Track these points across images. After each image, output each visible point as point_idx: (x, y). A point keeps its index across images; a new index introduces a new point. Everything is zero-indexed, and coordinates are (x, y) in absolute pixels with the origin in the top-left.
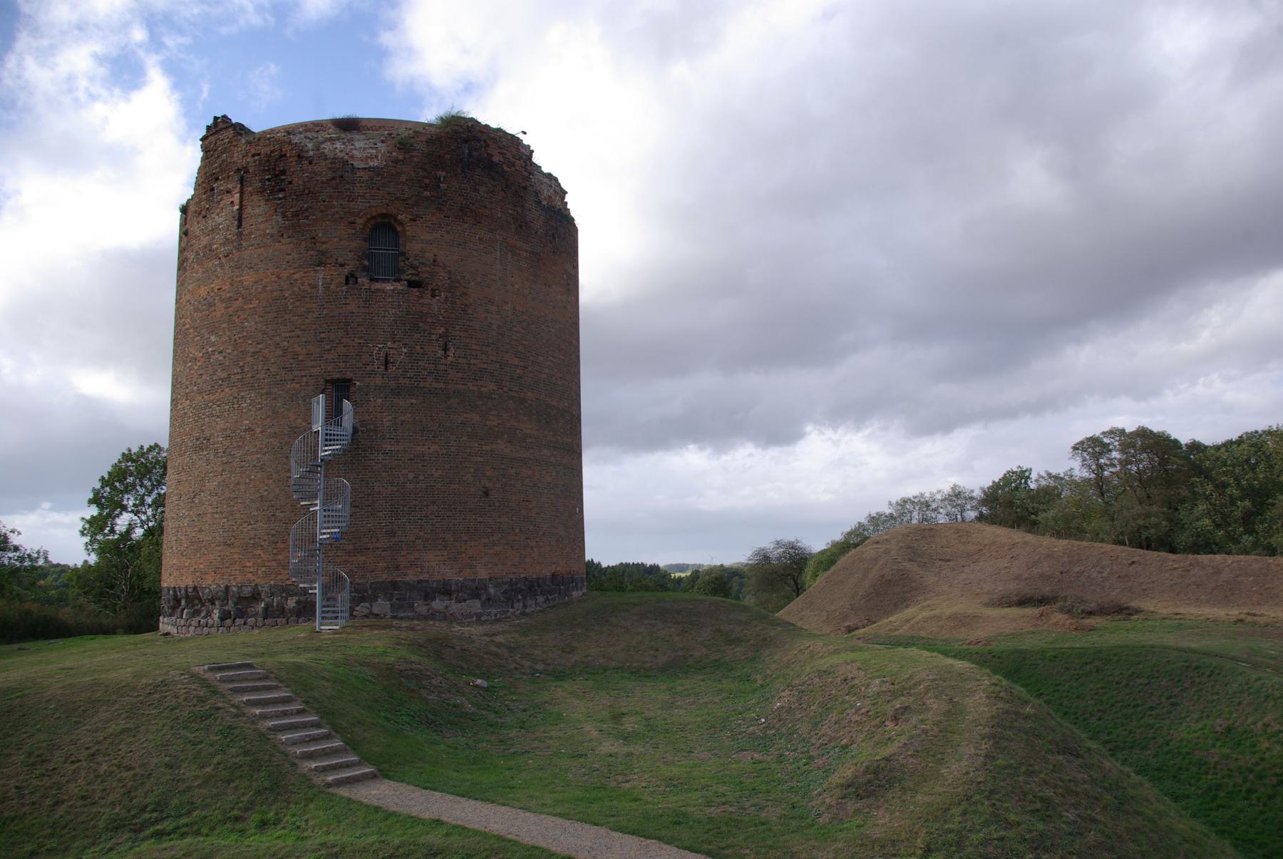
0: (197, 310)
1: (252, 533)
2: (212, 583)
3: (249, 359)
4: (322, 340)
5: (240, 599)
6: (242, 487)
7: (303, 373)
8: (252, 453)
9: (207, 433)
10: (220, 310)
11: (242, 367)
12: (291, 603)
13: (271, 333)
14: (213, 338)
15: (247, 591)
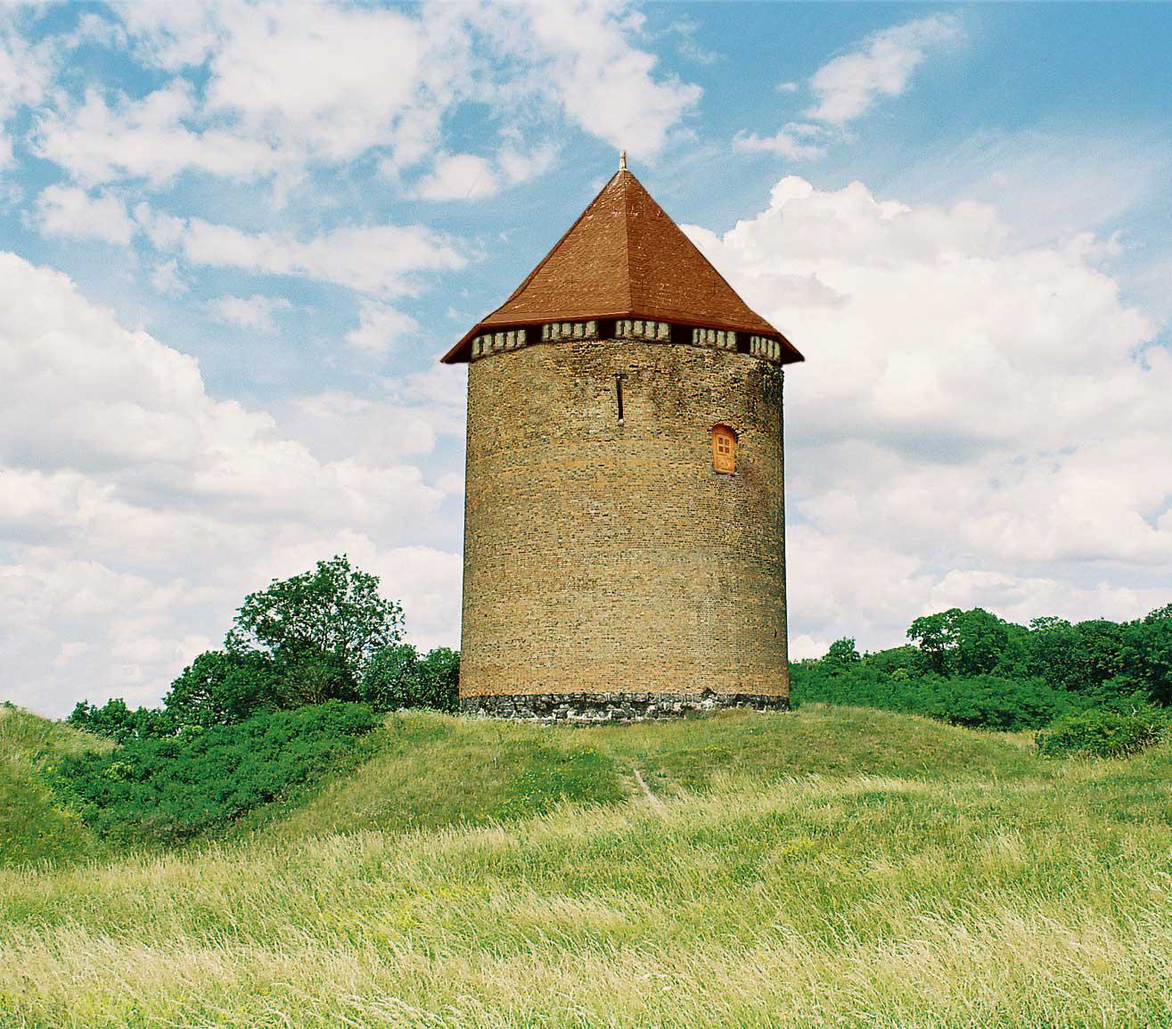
0: (573, 478)
1: (644, 655)
2: (605, 692)
3: (635, 523)
4: (693, 516)
5: (635, 704)
6: (633, 621)
7: (680, 539)
8: (642, 595)
9: (591, 576)
10: (603, 482)
11: (629, 530)
12: (677, 707)
13: (654, 506)
14: (596, 503)
15: (640, 698)
